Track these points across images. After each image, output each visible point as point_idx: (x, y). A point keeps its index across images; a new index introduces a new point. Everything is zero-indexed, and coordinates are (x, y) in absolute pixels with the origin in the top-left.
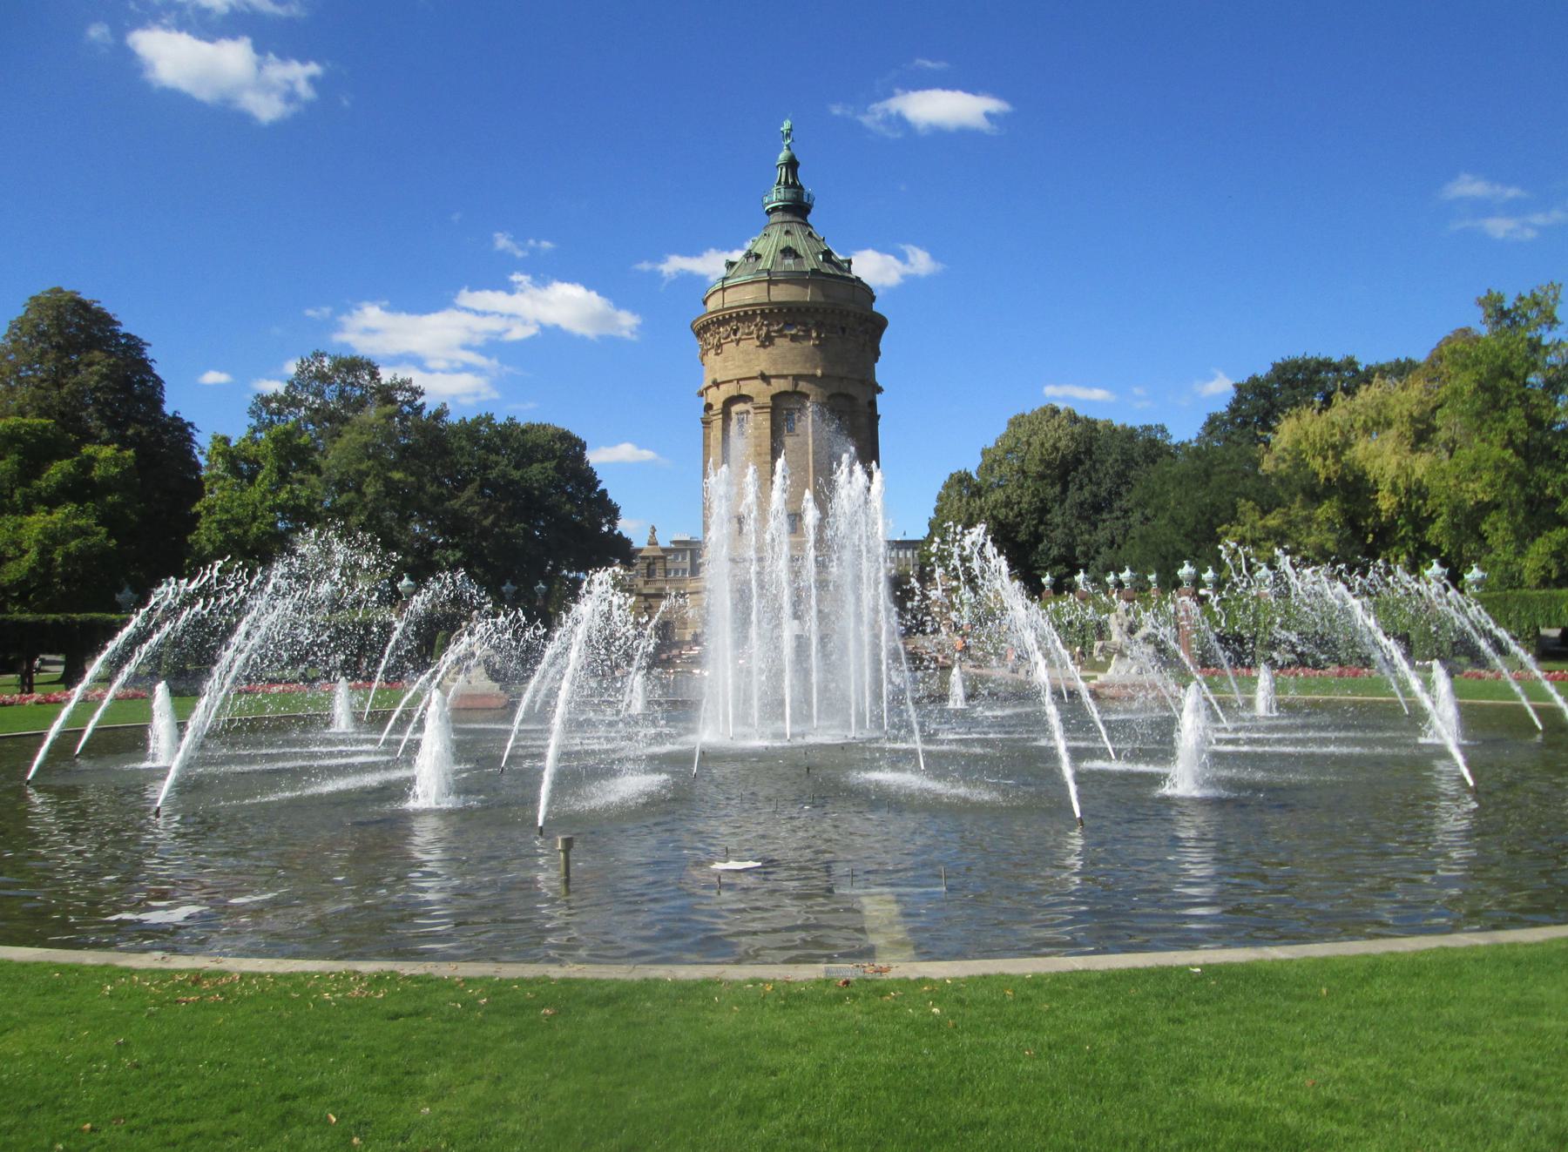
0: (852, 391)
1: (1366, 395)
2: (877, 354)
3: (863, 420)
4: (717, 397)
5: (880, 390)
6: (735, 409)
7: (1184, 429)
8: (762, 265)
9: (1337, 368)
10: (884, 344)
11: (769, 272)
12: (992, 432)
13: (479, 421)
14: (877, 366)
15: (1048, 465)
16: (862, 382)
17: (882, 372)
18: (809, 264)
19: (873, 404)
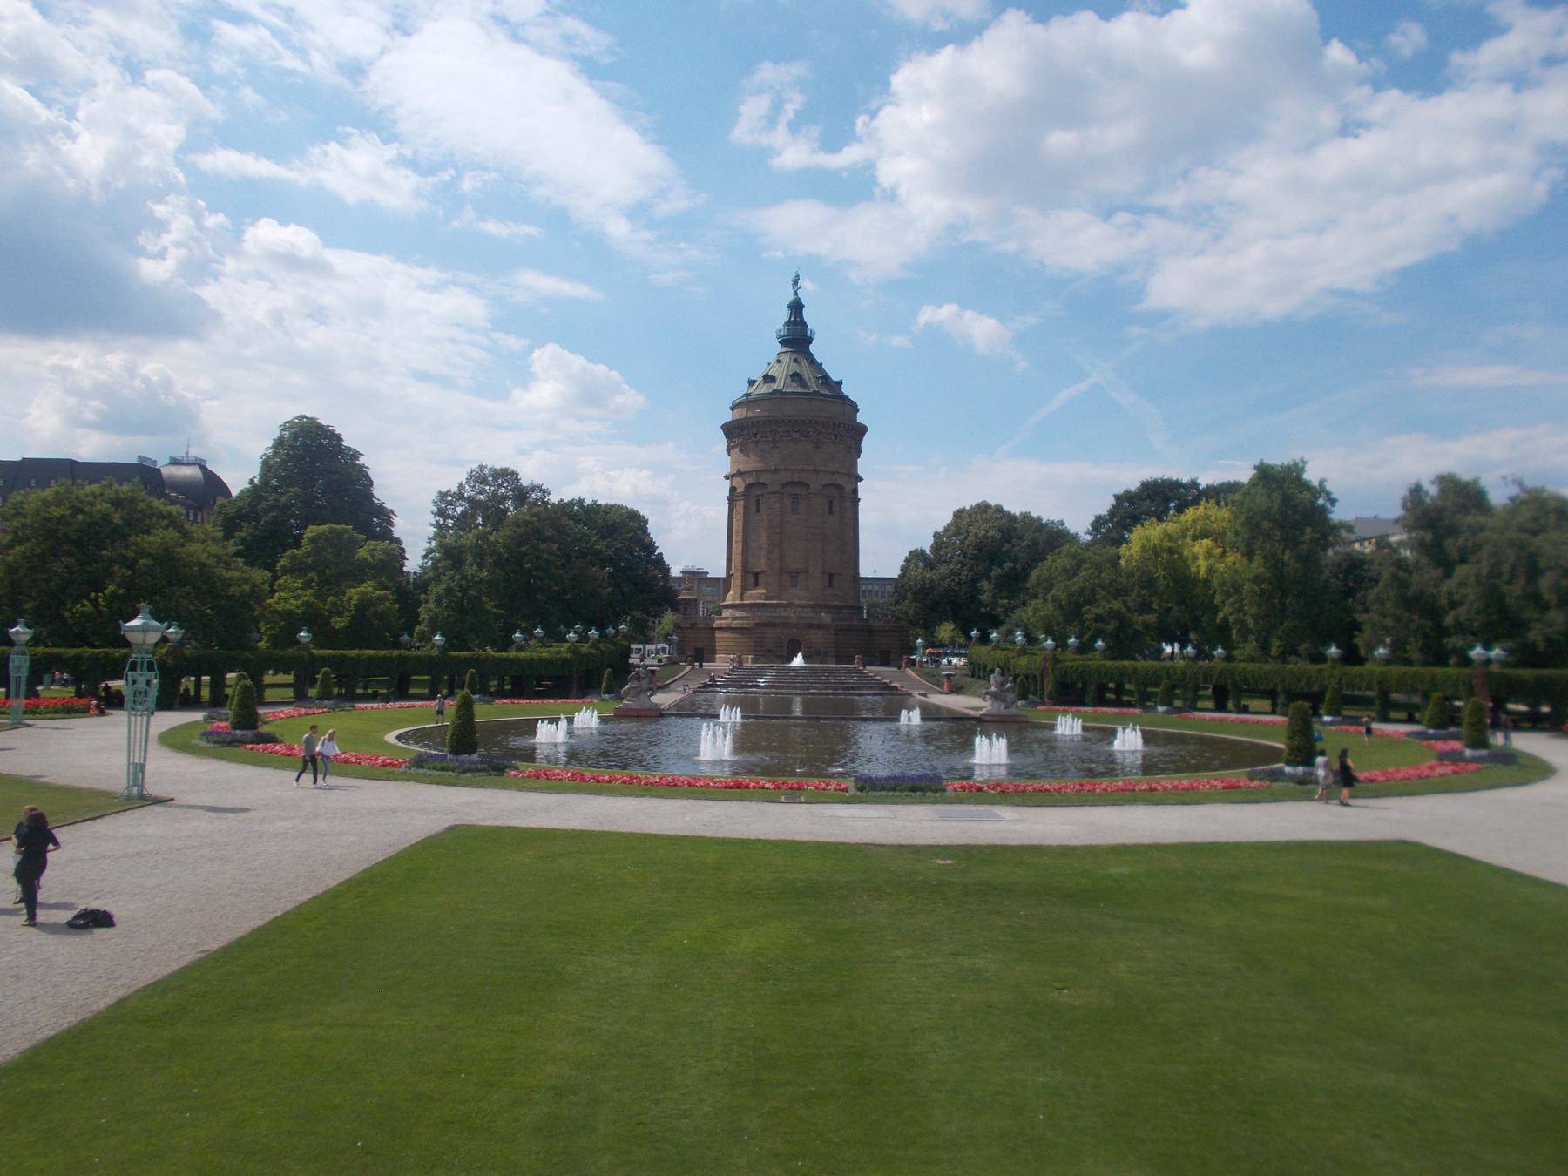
0: (840, 481)
1: (1190, 514)
2: (859, 452)
3: (848, 504)
4: (740, 486)
6: (757, 491)
7: (1079, 525)
8: (775, 387)
9: (1185, 486)
10: (864, 446)
11: (780, 392)
12: (943, 519)
13: (572, 503)
15: (980, 550)
16: (849, 475)
17: (863, 465)
18: (814, 388)
19: (855, 491)
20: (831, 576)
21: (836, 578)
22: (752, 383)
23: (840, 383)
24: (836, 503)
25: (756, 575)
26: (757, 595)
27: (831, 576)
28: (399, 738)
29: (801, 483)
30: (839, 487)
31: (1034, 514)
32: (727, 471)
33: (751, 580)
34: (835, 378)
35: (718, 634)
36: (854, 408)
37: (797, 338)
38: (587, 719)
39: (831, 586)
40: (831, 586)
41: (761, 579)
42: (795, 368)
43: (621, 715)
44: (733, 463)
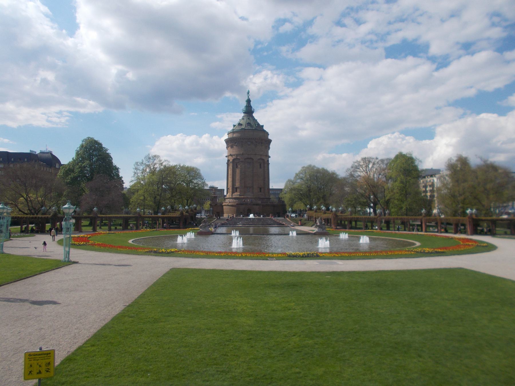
0: (263, 158)
2: (269, 148)
4: (231, 159)
5: (270, 157)
10: (271, 146)
11: (244, 129)
14: (269, 151)
17: (270, 153)
19: (268, 161)
20: (260, 188)
21: (262, 190)
22: (234, 126)
23: (263, 126)
24: (262, 165)
25: (236, 188)
26: (236, 194)
27: (260, 188)
28: (133, 242)
29: (250, 158)
30: (263, 159)
31: (325, 168)
32: (227, 155)
33: (235, 190)
34: (261, 124)
35: (224, 207)
36: (267, 134)
37: (249, 111)
38: (190, 235)
39: (260, 191)
40: (260, 191)
41: (238, 190)
42: (248, 121)
43: (200, 234)
44: (229, 151)
